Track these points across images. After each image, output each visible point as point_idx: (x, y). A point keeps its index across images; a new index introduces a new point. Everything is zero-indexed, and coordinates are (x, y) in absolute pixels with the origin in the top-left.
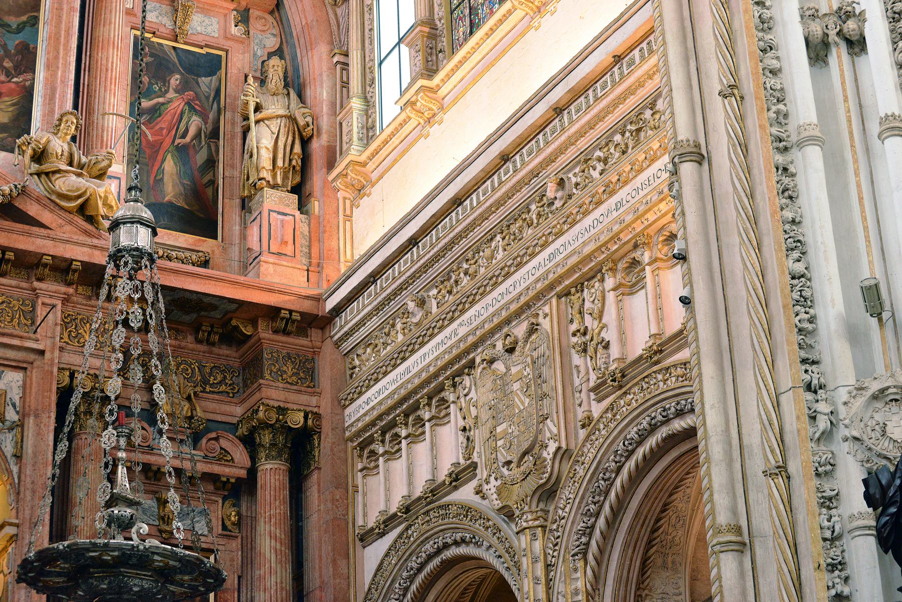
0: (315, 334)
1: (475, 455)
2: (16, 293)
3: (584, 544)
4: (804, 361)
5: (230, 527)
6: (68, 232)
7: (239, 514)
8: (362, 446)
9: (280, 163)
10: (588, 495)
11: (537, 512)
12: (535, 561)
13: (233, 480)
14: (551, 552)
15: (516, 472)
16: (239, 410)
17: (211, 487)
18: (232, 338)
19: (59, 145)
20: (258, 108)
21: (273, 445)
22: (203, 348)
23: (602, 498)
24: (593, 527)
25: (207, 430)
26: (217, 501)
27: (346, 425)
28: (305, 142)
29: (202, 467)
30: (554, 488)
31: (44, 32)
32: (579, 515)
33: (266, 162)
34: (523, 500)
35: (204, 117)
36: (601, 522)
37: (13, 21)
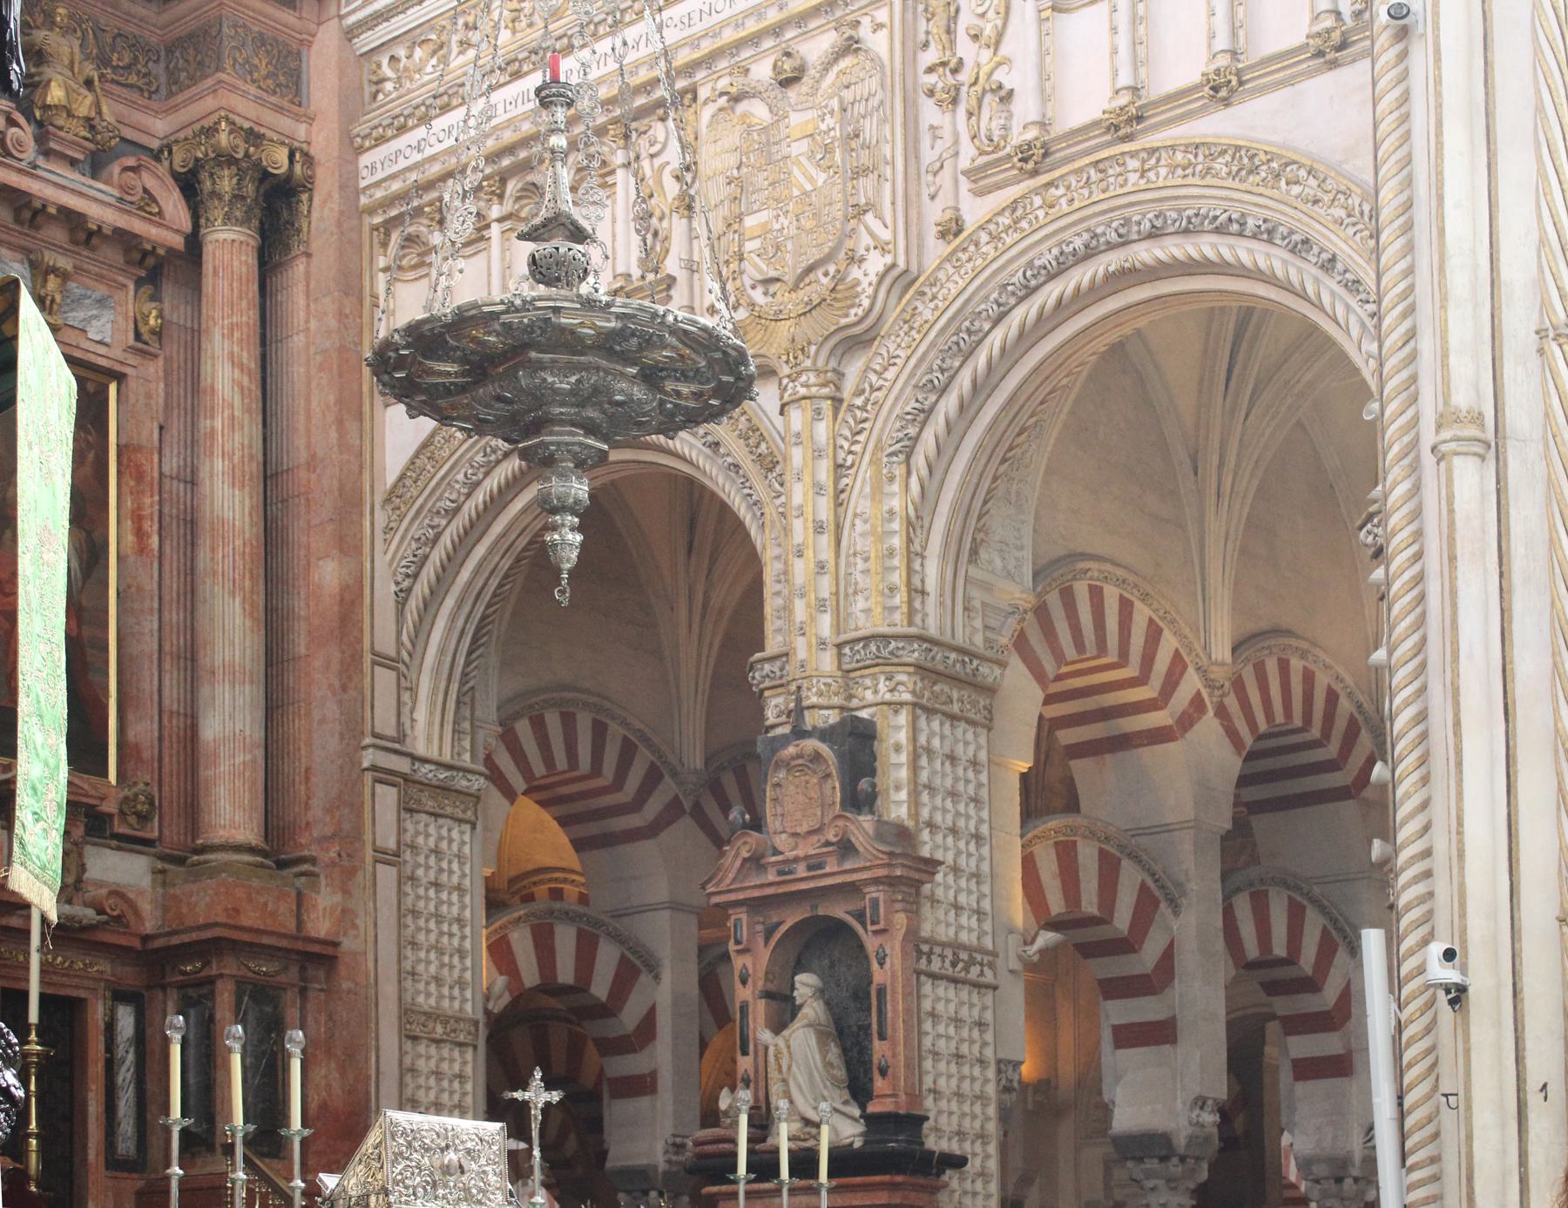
1: (672, 266)
3: (909, 439)
5: (146, 337)
10: (931, 355)
11: (826, 372)
12: (818, 454)
13: (161, 252)
14: (846, 445)
15: (791, 302)
21: (238, 197)
23: (957, 364)
24: (928, 413)
26: (125, 286)
27: (363, 184)
30: (872, 334)
32: (909, 389)
34: (802, 350)
36: (950, 403)
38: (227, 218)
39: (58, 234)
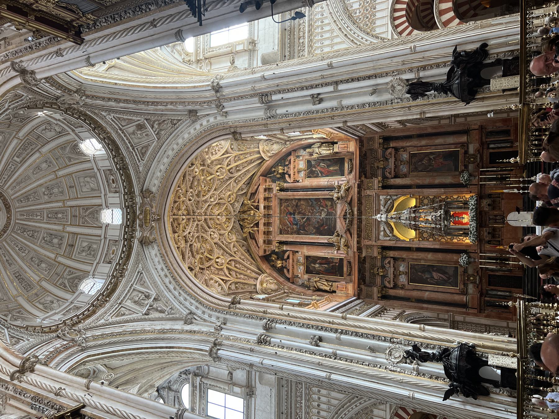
0: (362, 139)
2: (365, 199)
4: (386, 104)
6: (352, 192)
7: (402, 148)
8: (385, 128)
9: (328, 149)
16: (379, 150)
17: (397, 155)
18: (365, 155)
19: (336, 195)
20: (317, 153)
22: (368, 159)
25: (385, 158)
28: (322, 143)
29: (393, 158)
31: (311, 197)
33: (329, 152)
35: (320, 163)
37: (310, 203)
38: (390, 145)
39: (396, 163)
